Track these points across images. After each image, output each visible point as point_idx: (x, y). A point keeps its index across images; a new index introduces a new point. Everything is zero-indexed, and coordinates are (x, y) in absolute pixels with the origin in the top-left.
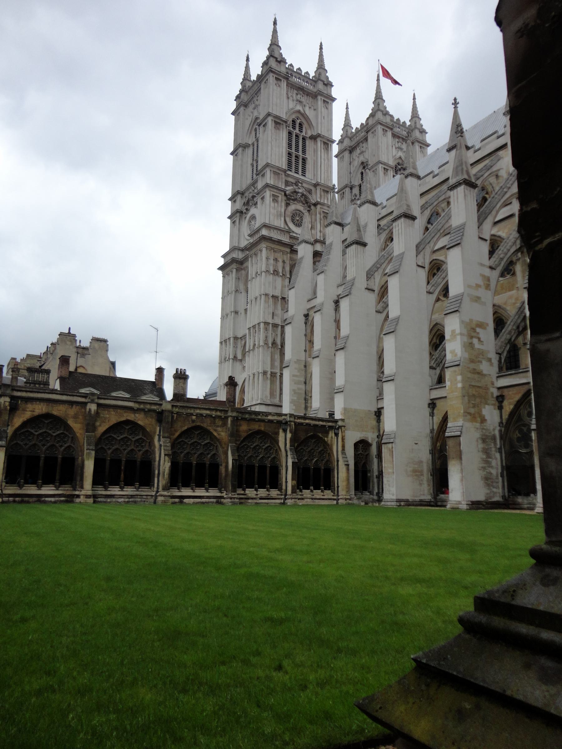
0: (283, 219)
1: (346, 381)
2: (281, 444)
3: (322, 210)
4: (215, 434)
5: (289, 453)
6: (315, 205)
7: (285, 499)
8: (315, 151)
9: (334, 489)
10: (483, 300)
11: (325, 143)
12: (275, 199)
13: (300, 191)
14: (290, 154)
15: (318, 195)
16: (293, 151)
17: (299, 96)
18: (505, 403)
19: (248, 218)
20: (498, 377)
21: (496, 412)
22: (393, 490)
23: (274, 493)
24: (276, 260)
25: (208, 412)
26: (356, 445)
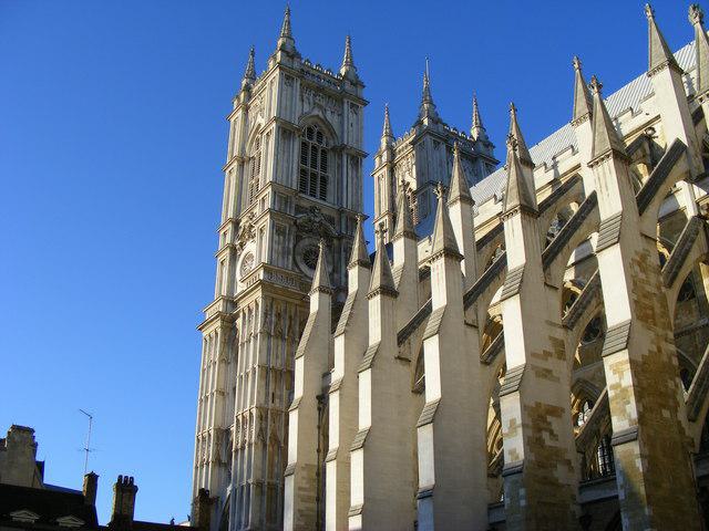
8: (340, 167)
10: (554, 374)
11: (353, 158)
12: (277, 230)
13: (317, 220)
15: (343, 226)
24: (279, 316)
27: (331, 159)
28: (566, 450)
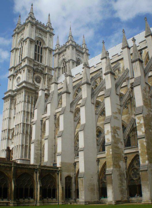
0: (32, 79)
1: (62, 150)
2: (35, 179)
3: (48, 77)
4: (6, 174)
5: (38, 183)
6: (46, 74)
7: (36, 203)
9: (57, 198)
12: (29, 71)
13: (39, 68)
14: (35, 54)
16: (37, 52)
17: (40, 32)
18: (128, 160)
19: (16, 78)
20: (124, 149)
21: (124, 164)
22: (83, 197)
23: (32, 200)
24: (29, 96)
25: (3, 165)
26: (66, 178)
27: (43, 50)
28: (121, 139)
